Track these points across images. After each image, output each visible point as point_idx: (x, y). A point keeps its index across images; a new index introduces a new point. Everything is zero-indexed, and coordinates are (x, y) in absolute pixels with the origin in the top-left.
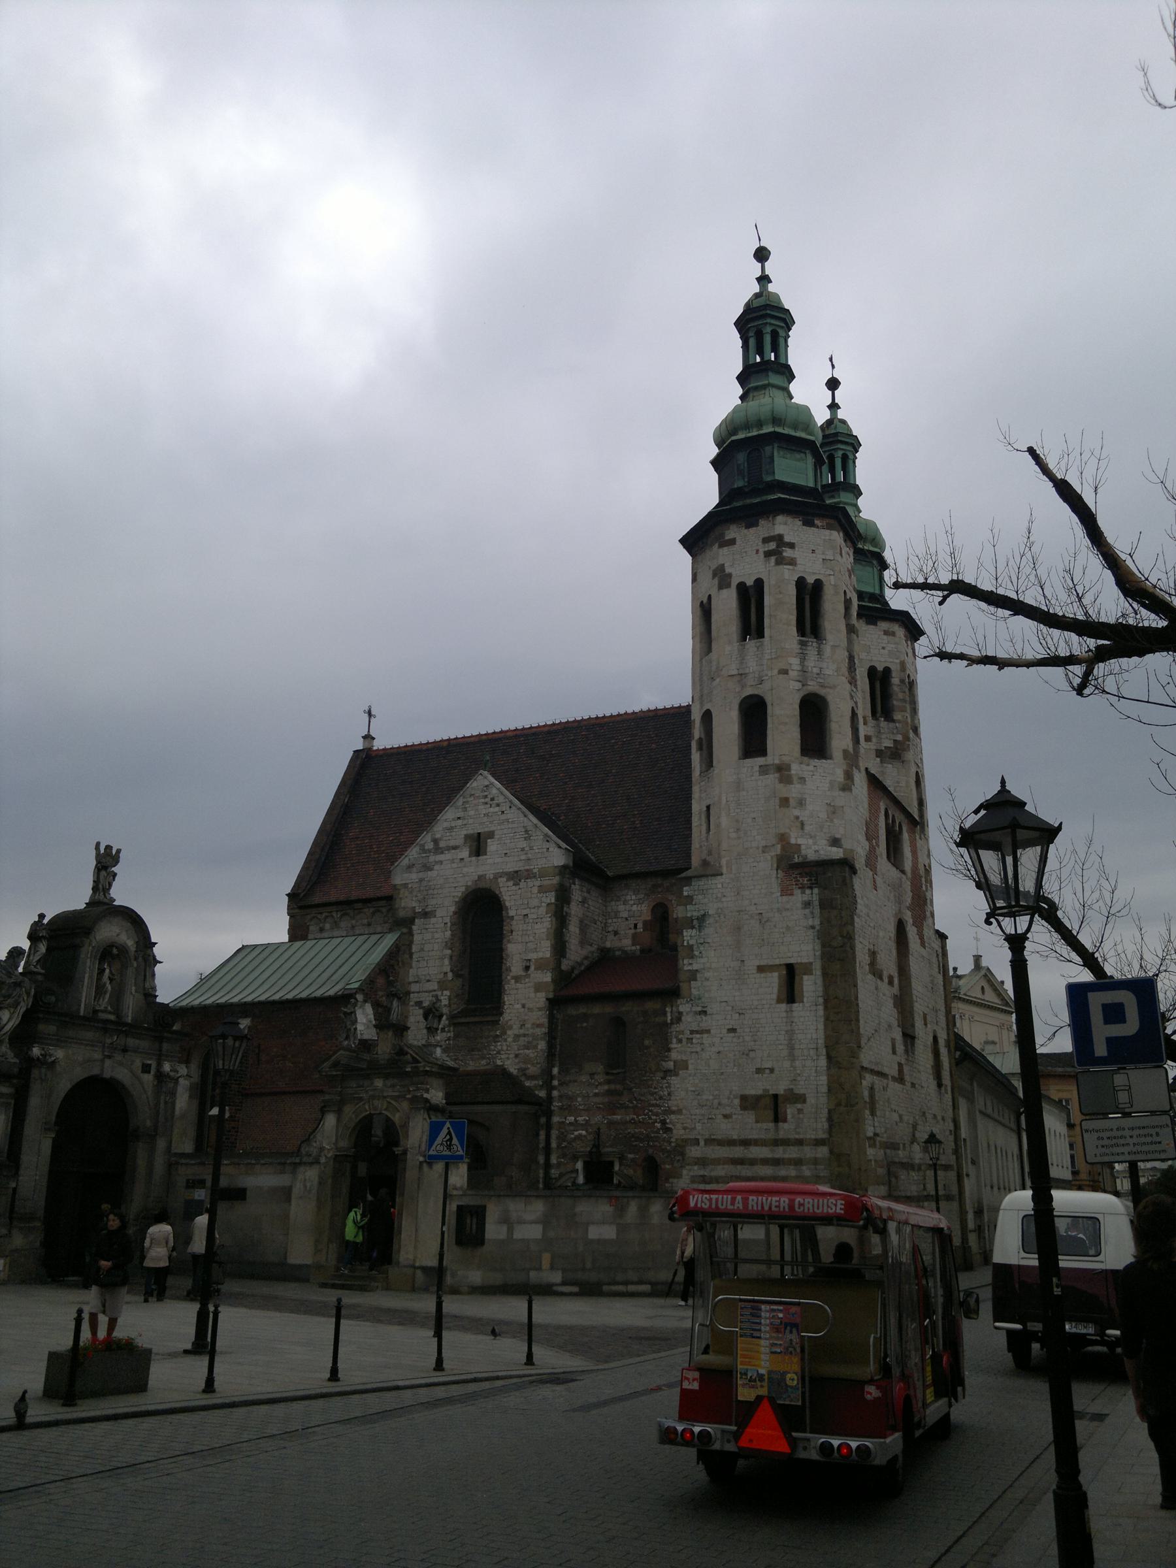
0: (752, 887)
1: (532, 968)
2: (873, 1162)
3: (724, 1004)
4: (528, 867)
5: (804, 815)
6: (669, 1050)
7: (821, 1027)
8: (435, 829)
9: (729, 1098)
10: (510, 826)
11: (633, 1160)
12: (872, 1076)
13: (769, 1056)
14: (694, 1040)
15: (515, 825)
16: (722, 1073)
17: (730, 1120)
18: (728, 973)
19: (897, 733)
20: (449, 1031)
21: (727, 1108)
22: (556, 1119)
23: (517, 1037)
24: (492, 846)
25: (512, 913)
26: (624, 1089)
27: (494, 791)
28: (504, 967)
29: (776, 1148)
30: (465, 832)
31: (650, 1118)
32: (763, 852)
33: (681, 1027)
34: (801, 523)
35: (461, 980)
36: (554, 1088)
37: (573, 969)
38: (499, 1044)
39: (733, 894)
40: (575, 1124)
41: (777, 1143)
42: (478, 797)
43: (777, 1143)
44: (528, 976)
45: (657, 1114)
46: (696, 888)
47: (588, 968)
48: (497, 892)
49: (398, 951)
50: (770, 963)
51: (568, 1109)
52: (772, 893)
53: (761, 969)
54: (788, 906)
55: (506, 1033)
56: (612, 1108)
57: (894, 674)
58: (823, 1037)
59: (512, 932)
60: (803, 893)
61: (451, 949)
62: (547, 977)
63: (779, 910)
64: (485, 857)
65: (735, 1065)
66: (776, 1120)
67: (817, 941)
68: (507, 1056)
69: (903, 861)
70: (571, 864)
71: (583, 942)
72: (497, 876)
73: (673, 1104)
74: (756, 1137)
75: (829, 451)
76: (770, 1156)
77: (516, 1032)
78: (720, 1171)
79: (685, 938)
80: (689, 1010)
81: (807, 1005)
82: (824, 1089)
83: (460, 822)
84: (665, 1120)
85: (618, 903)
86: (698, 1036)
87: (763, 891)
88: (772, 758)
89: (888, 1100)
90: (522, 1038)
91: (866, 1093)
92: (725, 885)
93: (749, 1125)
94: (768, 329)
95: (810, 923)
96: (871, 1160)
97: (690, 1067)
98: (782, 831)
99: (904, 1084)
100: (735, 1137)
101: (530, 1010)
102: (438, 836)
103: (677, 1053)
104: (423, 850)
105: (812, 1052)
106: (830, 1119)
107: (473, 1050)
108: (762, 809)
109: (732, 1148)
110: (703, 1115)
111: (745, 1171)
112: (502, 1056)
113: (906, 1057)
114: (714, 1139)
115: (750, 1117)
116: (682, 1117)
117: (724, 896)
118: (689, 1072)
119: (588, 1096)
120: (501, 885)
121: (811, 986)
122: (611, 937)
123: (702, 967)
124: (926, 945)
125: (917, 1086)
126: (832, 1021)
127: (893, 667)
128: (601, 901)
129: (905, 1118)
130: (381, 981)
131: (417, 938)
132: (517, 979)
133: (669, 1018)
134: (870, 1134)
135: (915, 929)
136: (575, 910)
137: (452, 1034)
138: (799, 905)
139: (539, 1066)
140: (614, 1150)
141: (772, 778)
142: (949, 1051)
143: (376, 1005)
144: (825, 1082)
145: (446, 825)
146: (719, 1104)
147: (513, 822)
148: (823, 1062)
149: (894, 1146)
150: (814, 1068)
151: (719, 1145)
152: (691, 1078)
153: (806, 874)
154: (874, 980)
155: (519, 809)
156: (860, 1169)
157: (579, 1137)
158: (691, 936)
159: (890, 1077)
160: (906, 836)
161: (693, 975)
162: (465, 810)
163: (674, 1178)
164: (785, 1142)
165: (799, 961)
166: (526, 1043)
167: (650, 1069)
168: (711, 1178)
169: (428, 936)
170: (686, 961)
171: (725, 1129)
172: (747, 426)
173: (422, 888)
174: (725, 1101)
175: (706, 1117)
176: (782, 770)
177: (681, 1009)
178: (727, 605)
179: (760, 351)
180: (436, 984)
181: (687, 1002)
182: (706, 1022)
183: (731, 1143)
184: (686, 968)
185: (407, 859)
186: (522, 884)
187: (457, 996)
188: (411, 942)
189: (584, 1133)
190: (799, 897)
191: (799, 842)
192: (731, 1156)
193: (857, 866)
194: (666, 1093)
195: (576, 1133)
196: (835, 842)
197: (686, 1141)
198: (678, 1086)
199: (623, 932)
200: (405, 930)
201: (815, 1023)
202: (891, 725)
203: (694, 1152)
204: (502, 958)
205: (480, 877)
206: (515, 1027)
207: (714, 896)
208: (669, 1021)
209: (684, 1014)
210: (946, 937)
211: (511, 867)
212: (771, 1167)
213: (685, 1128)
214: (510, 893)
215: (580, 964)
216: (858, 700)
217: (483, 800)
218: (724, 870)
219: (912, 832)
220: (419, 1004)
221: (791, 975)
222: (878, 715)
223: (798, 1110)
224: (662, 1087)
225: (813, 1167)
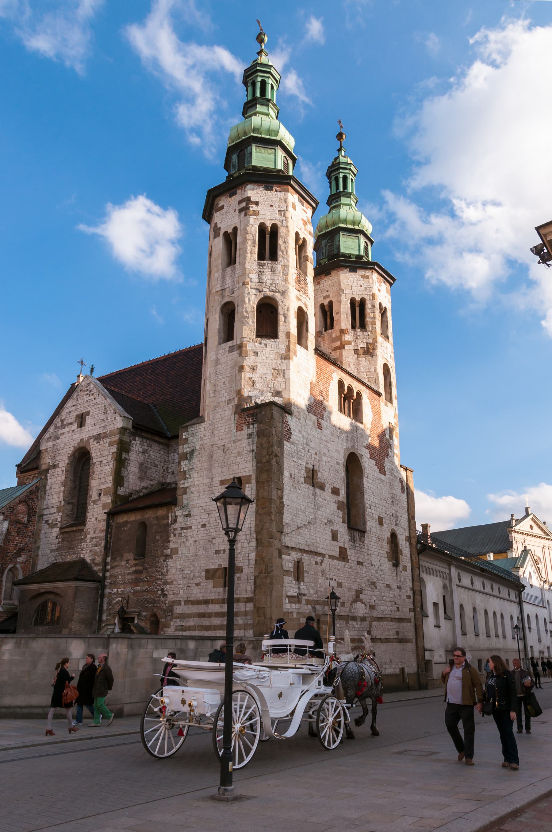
0: (221, 428)
2: (295, 615)
3: (201, 508)
4: (104, 431)
5: (256, 377)
6: (169, 542)
7: (254, 519)
8: (62, 414)
9: (199, 572)
10: (98, 406)
11: (145, 616)
12: (299, 554)
13: (223, 542)
14: (183, 535)
15: (100, 406)
16: (196, 555)
17: (199, 587)
18: (204, 487)
19: (369, 339)
20: (60, 538)
21: (198, 578)
22: (107, 591)
23: (92, 538)
25: (95, 461)
26: (144, 569)
27: (92, 386)
28: (88, 495)
29: (223, 605)
30: (76, 414)
31: (156, 588)
32: (228, 404)
33: (177, 526)
35: (71, 506)
36: (108, 571)
37: (130, 495)
38: (83, 544)
39: (209, 434)
40: (117, 594)
42: (84, 391)
44: (100, 500)
45: (159, 585)
46: (190, 432)
47: (146, 496)
48: (89, 449)
49: (38, 490)
50: (227, 479)
51: (114, 584)
52: (231, 431)
54: (240, 438)
55: (86, 537)
56: (136, 582)
57: (367, 302)
58: (254, 526)
59: (94, 472)
60: (248, 428)
61: (64, 486)
62: (108, 500)
63: (235, 442)
64: (84, 427)
65: (204, 549)
67: (255, 459)
68: (86, 551)
69: (362, 417)
70: (130, 426)
71: (141, 479)
72: (90, 438)
73: (168, 578)
74: (213, 598)
75: (333, 176)
76: (220, 611)
77: (91, 536)
78: (191, 622)
79: (182, 467)
80: (181, 514)
82: (253, 562)
83: (74, 407)
84: (163, 589)
85: (175, 454)
86: (185, 531)
87: (227, 430)
88: (236, 341)
89: (323, 572)
90: (94, 540)
91: (289, 566)
92: (206, 429)
95: (251, 448)
96: (292, 612)
97: (180, 552)
98: (239, 389)
99: (348, 561)
100: (201, 598)
101: (99, 521)
102: (63, 418)
104: (56, 428)
105: (248, 537)
106: (255, 583)
107: (70, 549)
108: (229, 375)
109: (199, 606)
110: (184, 584)
111: (206, 622)
112: (84, 552)
113: (351, 543)
114: (190, 600)
115: (210, 584)
116: (172, 586)
117: (205, 436)
118: (178, 555)
119: (125, 575)
120: (91, 444)
122: (170, 475)
123: (190, 484)
124: (387, 473)
125: (364, 564)
126: (260, 514)
128: (162, 453)
129: (346, 584)
130: (22, 508)
131: (49, 481)
132: (94, 502)
133: (170, 520)
134: (293, 592)
135: (374, 462)
137: (60, 540)
138: (246, 437)
139: (101, 557)
140: (136, 610)
141: (236, 353)
142: (410, 544)
143: (15, 522)
144: (254, 557)
145: (68, 410)
146: (194, 576)
148: (253, 543)
150: (248, 548)
151: (192, 604)
152: (179, 559)
153: (251, 414)
154: (312, 488)
155: (103, 395)
156: (271, 618)
157: (118, 602)
158: (185, 465)
159: (327, 556)
162: (77, 400)
163: (166, 627)
165: (244, 475)
166: (96, 543)
167: (158, 555)
168: (186, 627)
169: (54, 480)
170: (181, 482)
171: (197, 593)
173: (54, 451)
174: (197, 574)
175: (186, 586)
177: (177, 513)
180: (56, 509)
181: (181, 509)
182: (190, 521)
183: (198, 602)
184: (181, 487)
185: (48, 434)
186: (101, 442)
187: (68, 515)
188: (46, 484)
189: (120, 599)
190: (246, 431)
191: (251, 394)
192: (198, 612)
193: (294, 410)
194: (165, 570)
195: (117, 600)
197: (173, 602)
198: (172, 565)
199: (176, 472)
200: (43, 477)
201: (250, 516)
202: (366, 333)
203: (178, 610)
204: (88, 490)
205: (82, 440)
206: (92, 533)
207: (200, 437)
208: (170, 522)
209: (178, 517)
211: (96, 432)
212: (221, 619)
213: (174, 594)
214: (94, 449)
215: (138, 492)
216: (307, 303)
217: (86, 393)
218: (206, 419)
220: (47, 522)
222: (357, 328)
223: (238, 577)
225: (244, 617)
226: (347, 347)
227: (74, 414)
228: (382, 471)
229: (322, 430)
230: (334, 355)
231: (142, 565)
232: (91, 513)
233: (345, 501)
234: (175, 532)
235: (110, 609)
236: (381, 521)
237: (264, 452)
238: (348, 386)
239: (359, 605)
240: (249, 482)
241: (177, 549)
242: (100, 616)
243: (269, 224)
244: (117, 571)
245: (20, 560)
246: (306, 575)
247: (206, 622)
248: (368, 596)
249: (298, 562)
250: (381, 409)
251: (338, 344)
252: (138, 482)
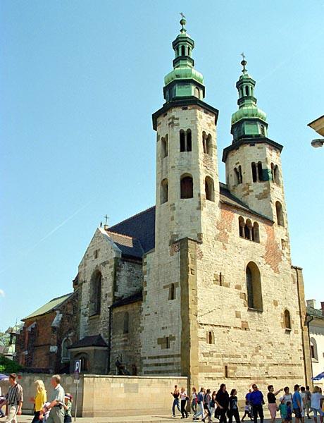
12: (211, 327)
24: (99, 253)
34: (181, 109)
37: (123, 296)
41: (166, 357)
43: (166, 357)
53: (165, 287)
62: (110, 299)
81: (177, 299)
88: (170, 201)
91: (204, 335)
93: (159, 350)
94: (180, 46)
111: (158, 368)
115: (160, 346)
127: (262, 161)
130: (70, 306)
142: (301, 317)
160: (262, 228)
164: (169, 356)
183: (155, 358)
196: (193, 231)
210: (300, 269)
221: (173, 287)
226: (250, 194)
227: (93, 251)
228: (276, 270)
229: (226, 249)
230: (243, 200)
231: (127, 336)
233: (246, 293)
236: (276, 304)
238: (247, 220)
239: (258, 356)
240: (178, 286)
241: (143, 327)
243: (185, 130)
244: (115, 340)
245: (69, 335)
246: (216, 339)
247: (158, 368)
248: (267, 350)
249: (210, 333)
250: (275, 231)
251: (245, 192)
252: (127, 288)
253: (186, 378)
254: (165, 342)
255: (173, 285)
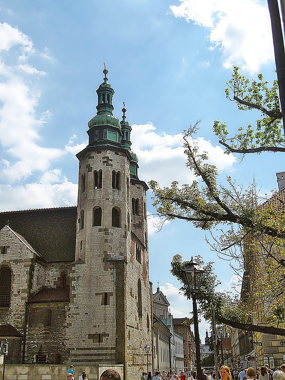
1: (21, 292)
6: (65, 320)
7: (115, 312)
16: (83, 327)
22: (27, 342)
24: (9, 251)
38: (8, 317)
41: (99, 349)
43: (99, 349)
47: (39, 292)
53: (96, 294)
55: (11, 313)
56: (46, 338)
62: (26, 295)
66: (99, 342)
71: (37, 285)
78: (81, 358)
79: (72, 284)
85: (50, 271)
92: (86, 267)
93: (91, 343)
103: (68, 320)
106: (116, 341)
111: (89, 358)
115: (91, 341)
121: (112, 299)
122: (47, 282)
132: (15, 296)
136: (35, 273)
146: (82, 337)
147: (16, 243)
149: (134, 349)
158: (74, 283)
161: (74, 296)
164: (102, 349)
171: (83, 345)
172: (99, 123)
176: (106, 230)
178: (91, 176)
179: (104, 100)
182: (78, 311)
183: (85, 349)
189: (36, 346)
190: (110, 271)
195: (34, 346)
196: (121, 254)
217: (6, 235)
219: (143, 251)
221: (106, 296)
224: (63, 332)
231: (50, 329)
232: (14, 301)
234: (69, 315)
235: (29, 351)
237: (121, 282)
242: (24, 354)
247: (89, 358)
253: (123, 365)
254: (99, 337)
255: (106, 294)
